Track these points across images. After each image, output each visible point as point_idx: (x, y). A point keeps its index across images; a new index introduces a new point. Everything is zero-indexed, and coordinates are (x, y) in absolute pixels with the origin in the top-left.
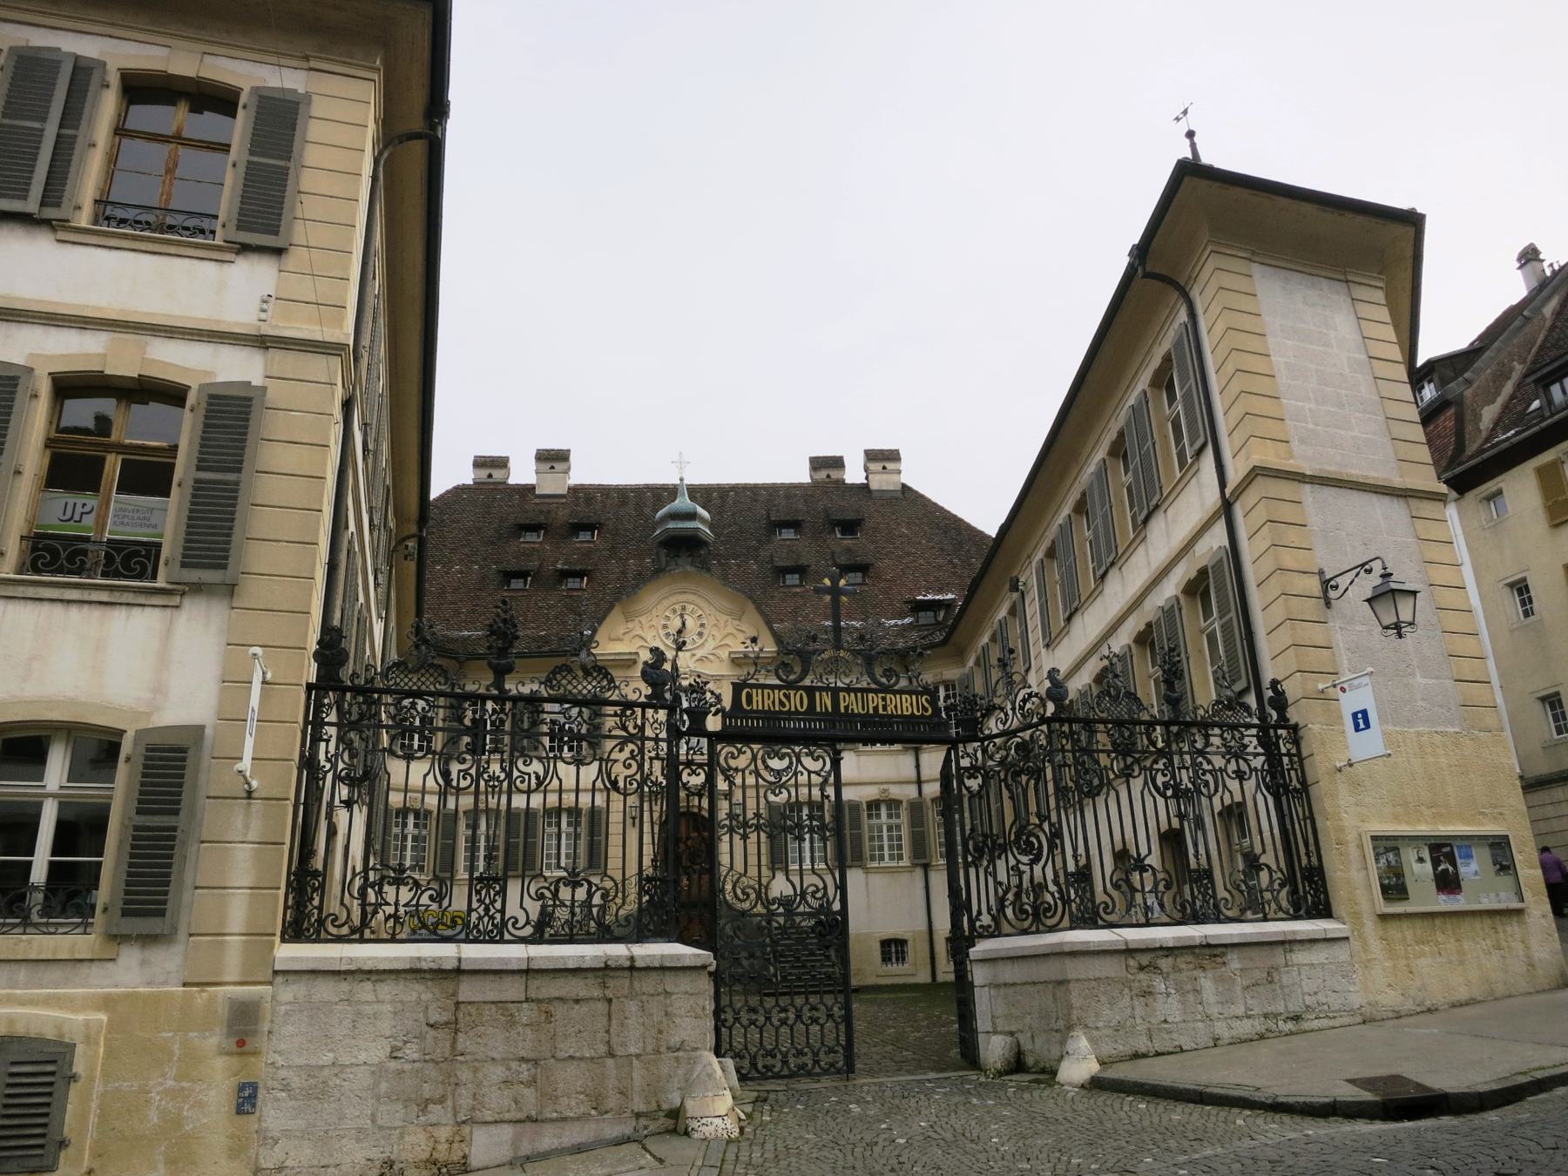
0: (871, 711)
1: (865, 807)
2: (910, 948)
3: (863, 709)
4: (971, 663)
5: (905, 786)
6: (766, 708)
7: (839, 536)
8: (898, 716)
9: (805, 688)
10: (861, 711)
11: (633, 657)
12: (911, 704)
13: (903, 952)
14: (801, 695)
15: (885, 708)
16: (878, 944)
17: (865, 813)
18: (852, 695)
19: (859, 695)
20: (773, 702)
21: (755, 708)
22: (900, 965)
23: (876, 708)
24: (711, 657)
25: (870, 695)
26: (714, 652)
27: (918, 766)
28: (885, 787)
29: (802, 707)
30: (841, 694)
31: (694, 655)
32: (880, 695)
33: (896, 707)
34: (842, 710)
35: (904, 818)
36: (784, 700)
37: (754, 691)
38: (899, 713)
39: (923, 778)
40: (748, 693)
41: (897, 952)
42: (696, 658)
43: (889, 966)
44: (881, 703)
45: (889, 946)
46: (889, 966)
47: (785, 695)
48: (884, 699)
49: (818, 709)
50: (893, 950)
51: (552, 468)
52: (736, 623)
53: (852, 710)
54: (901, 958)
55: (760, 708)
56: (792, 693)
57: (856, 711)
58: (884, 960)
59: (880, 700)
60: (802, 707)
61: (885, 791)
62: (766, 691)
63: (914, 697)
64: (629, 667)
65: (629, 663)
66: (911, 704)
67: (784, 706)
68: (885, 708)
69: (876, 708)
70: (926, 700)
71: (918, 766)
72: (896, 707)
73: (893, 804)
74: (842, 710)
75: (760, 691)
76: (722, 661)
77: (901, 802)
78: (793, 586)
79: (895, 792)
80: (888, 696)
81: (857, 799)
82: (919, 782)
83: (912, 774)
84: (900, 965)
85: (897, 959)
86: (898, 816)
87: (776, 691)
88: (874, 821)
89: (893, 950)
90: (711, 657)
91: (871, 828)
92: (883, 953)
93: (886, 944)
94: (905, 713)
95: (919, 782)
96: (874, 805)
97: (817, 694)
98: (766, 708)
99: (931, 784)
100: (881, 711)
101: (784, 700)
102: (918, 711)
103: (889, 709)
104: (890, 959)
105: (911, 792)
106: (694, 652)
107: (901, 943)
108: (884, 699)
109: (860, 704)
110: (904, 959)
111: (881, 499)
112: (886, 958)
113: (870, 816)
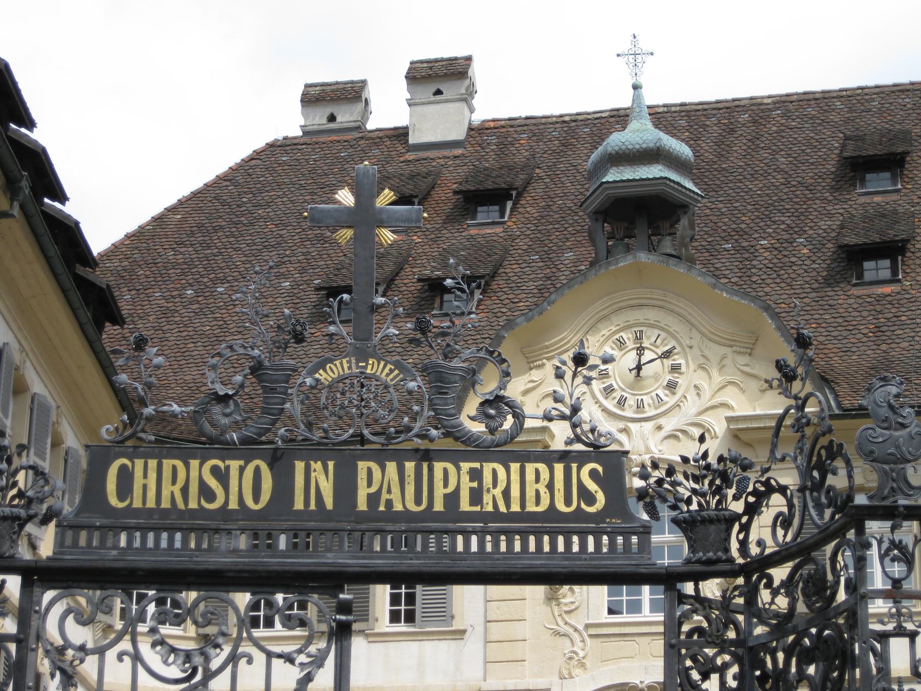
12: (550, 486)
15: (476, 496)
18: (392, 467)
19: (410, 466)
23: (452, 499)
25: (439, 467)
33: (506, 493)
38: (515, 507)
44: (467, 484)
48: (476, 475)
59: (465, 478)
63: (559, 468)
66: (550, 486)
68: (476, 496)
69: (452, 499)
70: (593, 474)
72: (506, 493)
94: (531, 508)
100: (465, 505)
102: (568, 502)
103: (487, 499)
108: (476, 475)
109: (410, 489)
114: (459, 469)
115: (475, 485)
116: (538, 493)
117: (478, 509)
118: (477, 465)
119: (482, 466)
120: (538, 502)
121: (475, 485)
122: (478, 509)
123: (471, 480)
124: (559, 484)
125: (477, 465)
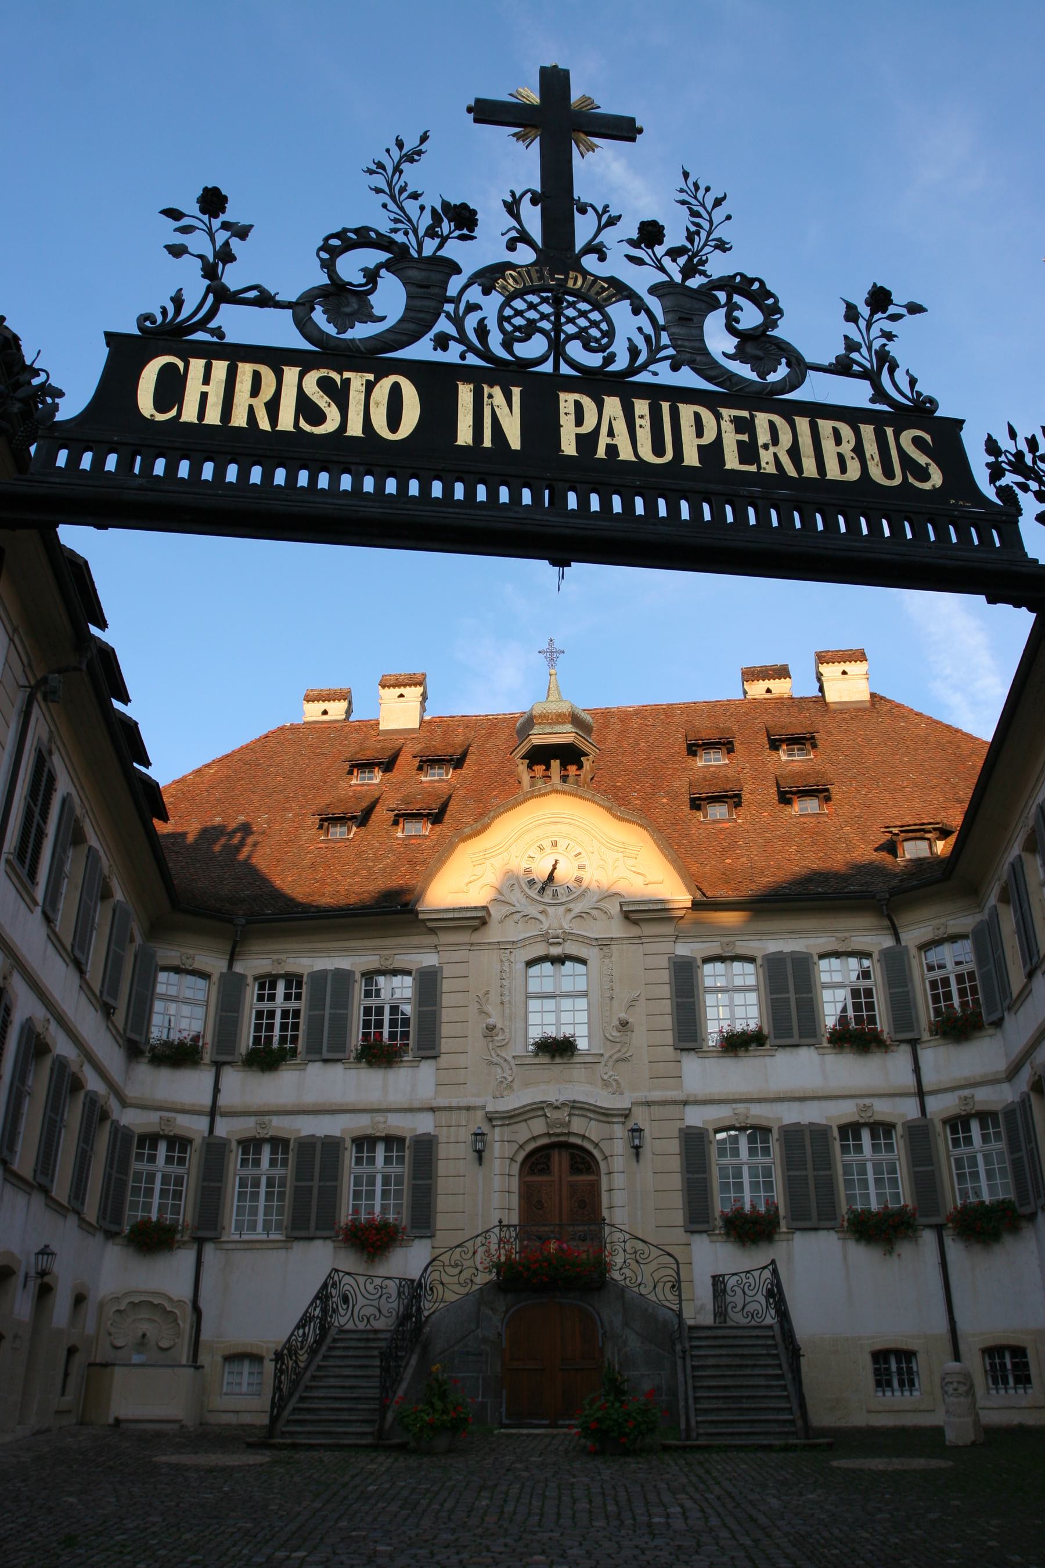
0: (691, 458)
1: (836, 1133)
2: (920, 1365)
3: (658, 449)
4: (993, 900)
5: (898, 1100)
6: (239, 420)
7: (784, 758)
8: (803, 482)
9: (414, 370)
10: (646, 453)
11: (480, 914)
12: (859, 450)
13: (910, 1370)
14: (396, 392)
15: (748, 452)
16: (868, 1360)
17: (837, 1144)
19: (642, 407)
20: (273, 407)
21: (190, 414)
22: (907, 1393)
23: (712, 452)
24: (594, 912)
26: (596, 905)
27: (917, 1070)
28: (867, 1101)
29: (394, 422)
30: (567, 401)
31: (570, 910)
32: (726, 413)
33: (794, 453)
34: (569, 447)
35: (900, 1152)
36: (321, 400)
37: (197, 366)
39: (926, 1088)
40: (167, 371)
41: (900, 1370)
42: (572, 914)
43: (888, 1394)
44: (731, 440)
45: (887, 1361)
46: (888, 1394)
47: (324, 384)
48: (744, 426)
49: (464, 436)
50: (894, 1367)
51: (401, 696)
52: (630, 862)
53: (612, 449)
54: (908, 1380)
55: (213, 417)
56: (357, 381)
57: (626, 453)
58: (879, 1384)
59: (727, 427)
60: (394, 422)
61: (866, 1108)
62: (245, 371)
64: (475, 929)
65: (476, 923)
66: (859, 450)
67: (317, 416)
68: (748, 452)
69: (712, 452)
71: (917, 1070)
72: (794, 453)
73: (882, 1130)
74: (569, 447)
75: (220, 368)
76: (611, 917)
77: (893, 1126)
78: (718, 821)
79: (884, 1110)
80: (762, 419)
81: (824, 1122)
82: (921, 1093)
83: (908, 1080)
84: (907, 1393)
85: (902, 1384)
86: (889, 1147)
87: (291, 374)
88: (852, 1157)
89: (894, 1367)
90: (594, 912)
91: (847, 1168)
92: (877, 1372)
93: (880, 1357)
95: (921, 1093)
96: (850, 1131)
97: (465, 394)
98: (239, 420)
99: (940, 1096)
100: (732, 461)
101: (321, 400)
102: (889, 473)
103: (766, 457)
104: (889, 1384)
105: (910, 1109)
106: (571, 906)
107: (906, 1355)
108: (744, 426)
109: (644, 436)
110: (912, 1384)
111: (841, 711)
112: (882, 1382)
113: (845, 1149)
114: (718, 417)
115: (745, 437)
116: (841, 458)
117: (753, 468)
118: (745, 414)
119: (752, 416)
120: (843, 469)
121: (745, 437)
122: (753, 468)
123: (738, 431)
124: (871, 448)
125: (745, 414)
